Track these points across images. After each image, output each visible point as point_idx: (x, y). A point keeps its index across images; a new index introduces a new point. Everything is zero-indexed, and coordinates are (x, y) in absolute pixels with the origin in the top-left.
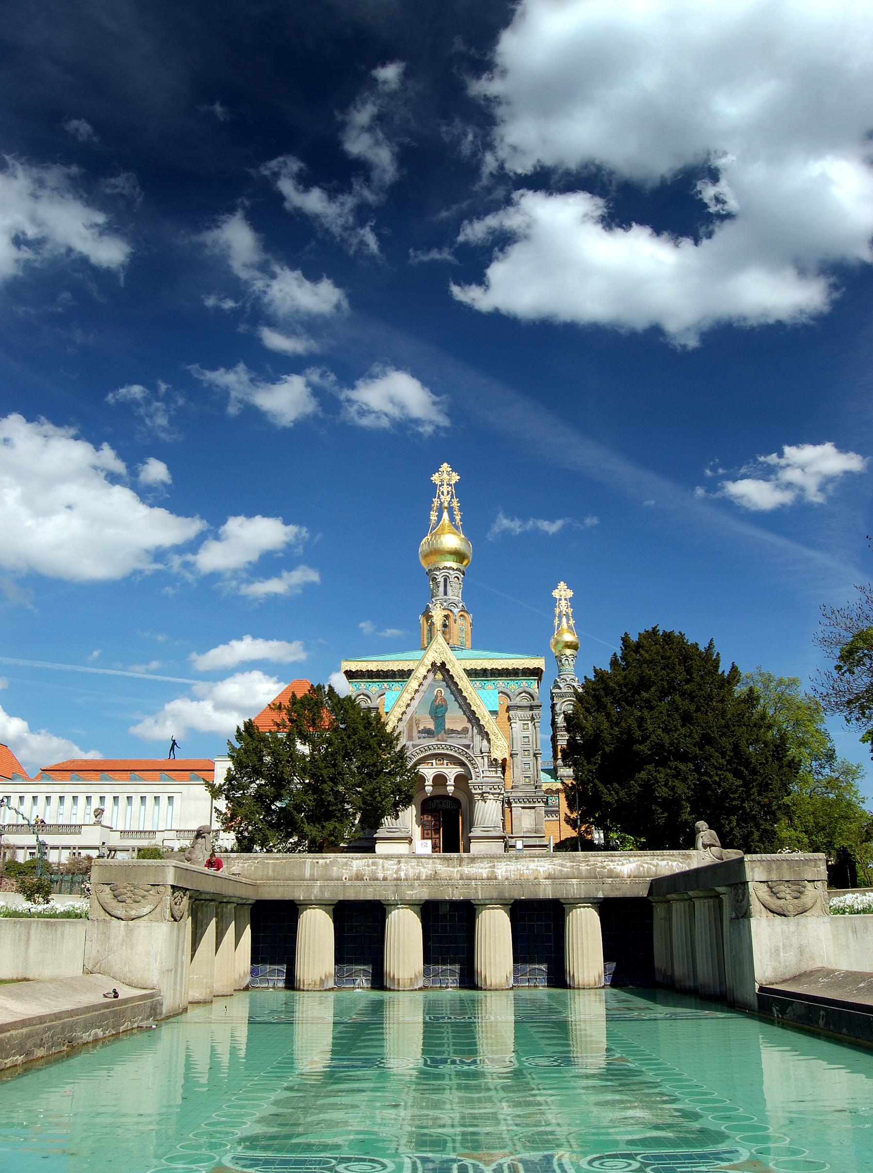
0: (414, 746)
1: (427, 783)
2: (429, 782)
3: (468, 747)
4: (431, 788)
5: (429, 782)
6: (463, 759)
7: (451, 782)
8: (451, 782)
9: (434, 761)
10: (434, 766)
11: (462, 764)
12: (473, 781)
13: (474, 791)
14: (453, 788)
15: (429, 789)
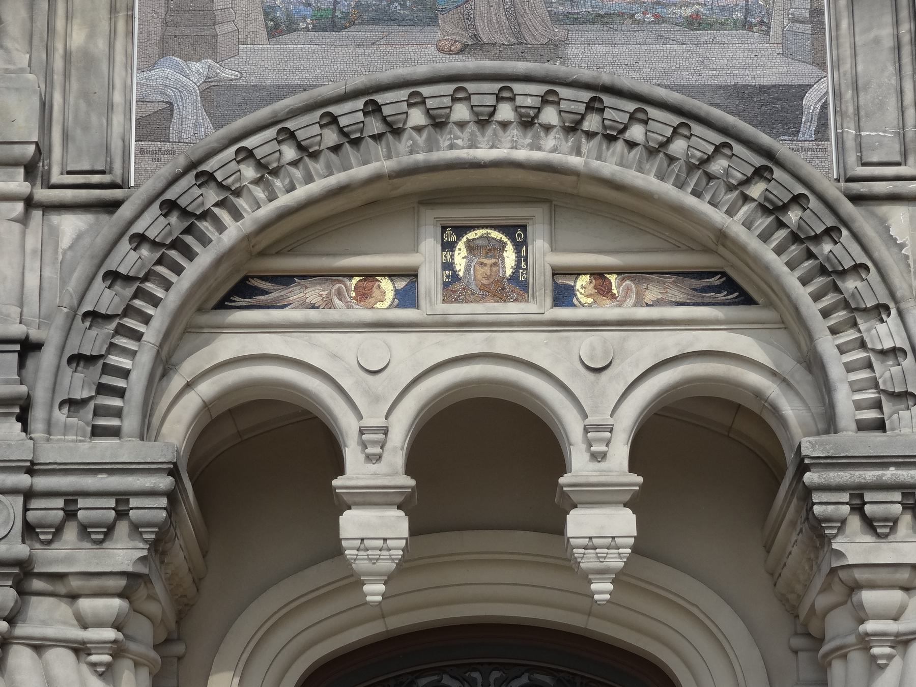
0: (214, 96)
1: (357, 471)
2: (374, 463)
3: (779, 106)
4: (394, 525)
5: (374, 463)
6: (740, 226)
7: (599, 457)
8: (599, 457)
9: (427, 256)
10: (432, 303)
11: (726, 284)
12: (850, 440)
13: (855, 547)
14: (623, 523)
15: (373, 531)
